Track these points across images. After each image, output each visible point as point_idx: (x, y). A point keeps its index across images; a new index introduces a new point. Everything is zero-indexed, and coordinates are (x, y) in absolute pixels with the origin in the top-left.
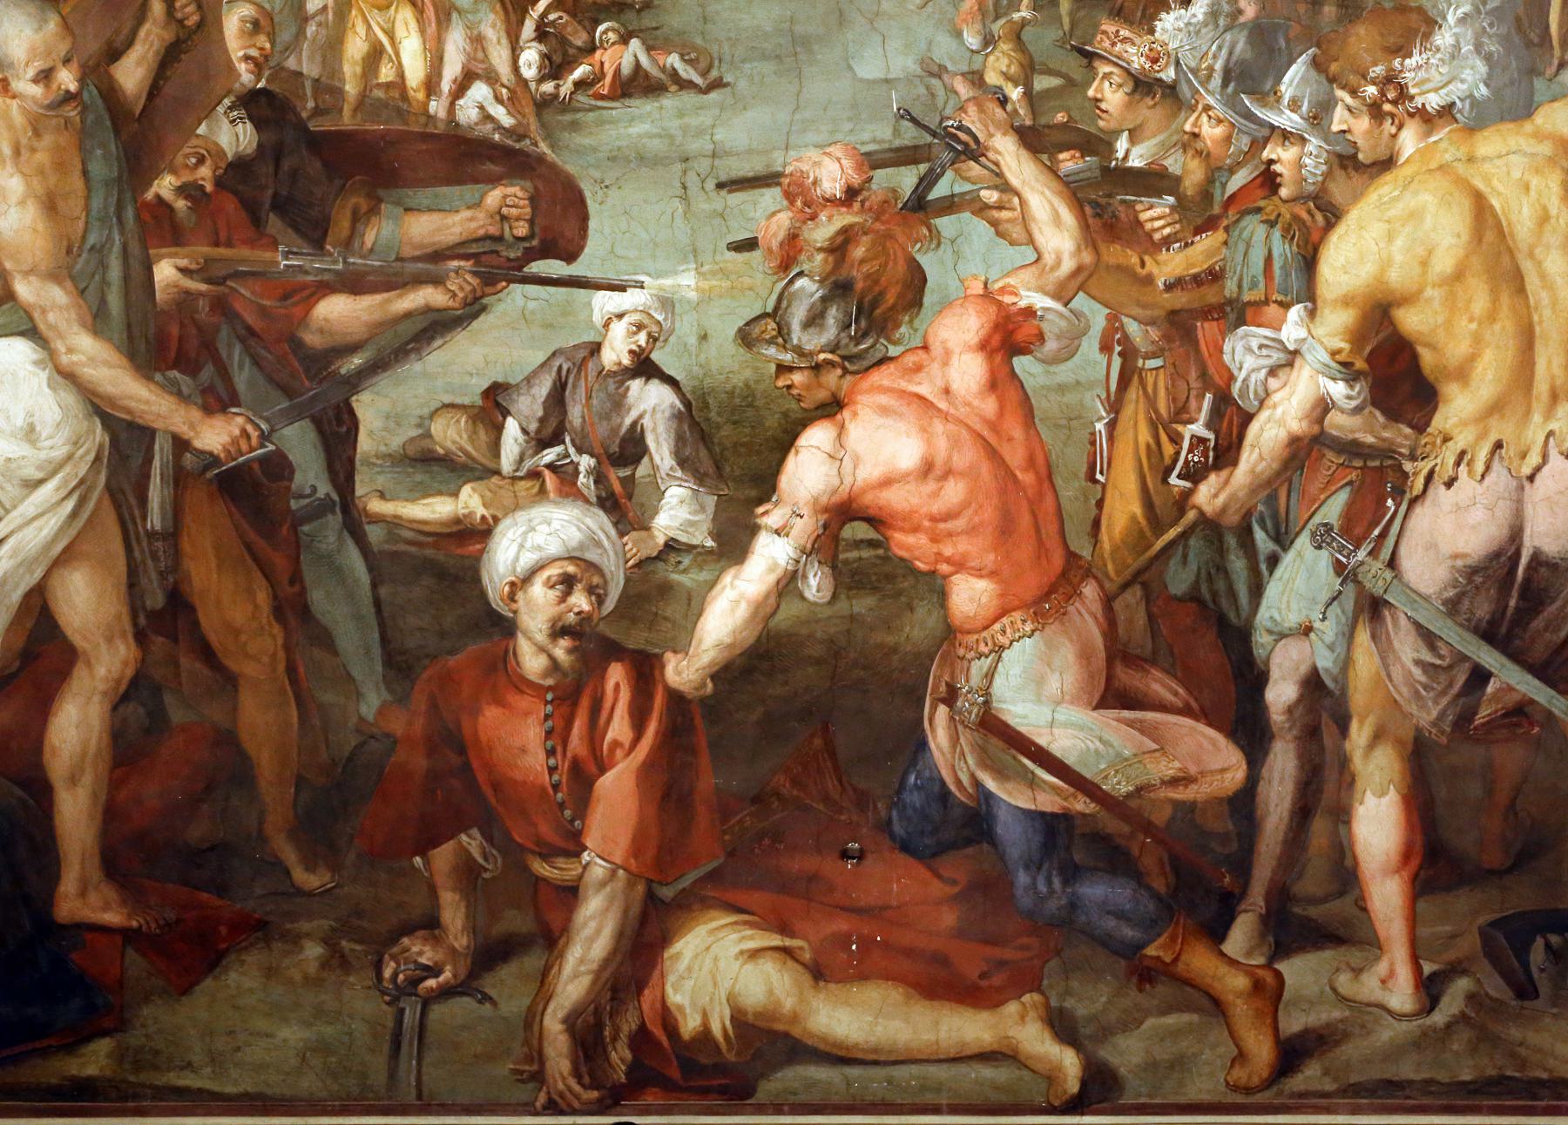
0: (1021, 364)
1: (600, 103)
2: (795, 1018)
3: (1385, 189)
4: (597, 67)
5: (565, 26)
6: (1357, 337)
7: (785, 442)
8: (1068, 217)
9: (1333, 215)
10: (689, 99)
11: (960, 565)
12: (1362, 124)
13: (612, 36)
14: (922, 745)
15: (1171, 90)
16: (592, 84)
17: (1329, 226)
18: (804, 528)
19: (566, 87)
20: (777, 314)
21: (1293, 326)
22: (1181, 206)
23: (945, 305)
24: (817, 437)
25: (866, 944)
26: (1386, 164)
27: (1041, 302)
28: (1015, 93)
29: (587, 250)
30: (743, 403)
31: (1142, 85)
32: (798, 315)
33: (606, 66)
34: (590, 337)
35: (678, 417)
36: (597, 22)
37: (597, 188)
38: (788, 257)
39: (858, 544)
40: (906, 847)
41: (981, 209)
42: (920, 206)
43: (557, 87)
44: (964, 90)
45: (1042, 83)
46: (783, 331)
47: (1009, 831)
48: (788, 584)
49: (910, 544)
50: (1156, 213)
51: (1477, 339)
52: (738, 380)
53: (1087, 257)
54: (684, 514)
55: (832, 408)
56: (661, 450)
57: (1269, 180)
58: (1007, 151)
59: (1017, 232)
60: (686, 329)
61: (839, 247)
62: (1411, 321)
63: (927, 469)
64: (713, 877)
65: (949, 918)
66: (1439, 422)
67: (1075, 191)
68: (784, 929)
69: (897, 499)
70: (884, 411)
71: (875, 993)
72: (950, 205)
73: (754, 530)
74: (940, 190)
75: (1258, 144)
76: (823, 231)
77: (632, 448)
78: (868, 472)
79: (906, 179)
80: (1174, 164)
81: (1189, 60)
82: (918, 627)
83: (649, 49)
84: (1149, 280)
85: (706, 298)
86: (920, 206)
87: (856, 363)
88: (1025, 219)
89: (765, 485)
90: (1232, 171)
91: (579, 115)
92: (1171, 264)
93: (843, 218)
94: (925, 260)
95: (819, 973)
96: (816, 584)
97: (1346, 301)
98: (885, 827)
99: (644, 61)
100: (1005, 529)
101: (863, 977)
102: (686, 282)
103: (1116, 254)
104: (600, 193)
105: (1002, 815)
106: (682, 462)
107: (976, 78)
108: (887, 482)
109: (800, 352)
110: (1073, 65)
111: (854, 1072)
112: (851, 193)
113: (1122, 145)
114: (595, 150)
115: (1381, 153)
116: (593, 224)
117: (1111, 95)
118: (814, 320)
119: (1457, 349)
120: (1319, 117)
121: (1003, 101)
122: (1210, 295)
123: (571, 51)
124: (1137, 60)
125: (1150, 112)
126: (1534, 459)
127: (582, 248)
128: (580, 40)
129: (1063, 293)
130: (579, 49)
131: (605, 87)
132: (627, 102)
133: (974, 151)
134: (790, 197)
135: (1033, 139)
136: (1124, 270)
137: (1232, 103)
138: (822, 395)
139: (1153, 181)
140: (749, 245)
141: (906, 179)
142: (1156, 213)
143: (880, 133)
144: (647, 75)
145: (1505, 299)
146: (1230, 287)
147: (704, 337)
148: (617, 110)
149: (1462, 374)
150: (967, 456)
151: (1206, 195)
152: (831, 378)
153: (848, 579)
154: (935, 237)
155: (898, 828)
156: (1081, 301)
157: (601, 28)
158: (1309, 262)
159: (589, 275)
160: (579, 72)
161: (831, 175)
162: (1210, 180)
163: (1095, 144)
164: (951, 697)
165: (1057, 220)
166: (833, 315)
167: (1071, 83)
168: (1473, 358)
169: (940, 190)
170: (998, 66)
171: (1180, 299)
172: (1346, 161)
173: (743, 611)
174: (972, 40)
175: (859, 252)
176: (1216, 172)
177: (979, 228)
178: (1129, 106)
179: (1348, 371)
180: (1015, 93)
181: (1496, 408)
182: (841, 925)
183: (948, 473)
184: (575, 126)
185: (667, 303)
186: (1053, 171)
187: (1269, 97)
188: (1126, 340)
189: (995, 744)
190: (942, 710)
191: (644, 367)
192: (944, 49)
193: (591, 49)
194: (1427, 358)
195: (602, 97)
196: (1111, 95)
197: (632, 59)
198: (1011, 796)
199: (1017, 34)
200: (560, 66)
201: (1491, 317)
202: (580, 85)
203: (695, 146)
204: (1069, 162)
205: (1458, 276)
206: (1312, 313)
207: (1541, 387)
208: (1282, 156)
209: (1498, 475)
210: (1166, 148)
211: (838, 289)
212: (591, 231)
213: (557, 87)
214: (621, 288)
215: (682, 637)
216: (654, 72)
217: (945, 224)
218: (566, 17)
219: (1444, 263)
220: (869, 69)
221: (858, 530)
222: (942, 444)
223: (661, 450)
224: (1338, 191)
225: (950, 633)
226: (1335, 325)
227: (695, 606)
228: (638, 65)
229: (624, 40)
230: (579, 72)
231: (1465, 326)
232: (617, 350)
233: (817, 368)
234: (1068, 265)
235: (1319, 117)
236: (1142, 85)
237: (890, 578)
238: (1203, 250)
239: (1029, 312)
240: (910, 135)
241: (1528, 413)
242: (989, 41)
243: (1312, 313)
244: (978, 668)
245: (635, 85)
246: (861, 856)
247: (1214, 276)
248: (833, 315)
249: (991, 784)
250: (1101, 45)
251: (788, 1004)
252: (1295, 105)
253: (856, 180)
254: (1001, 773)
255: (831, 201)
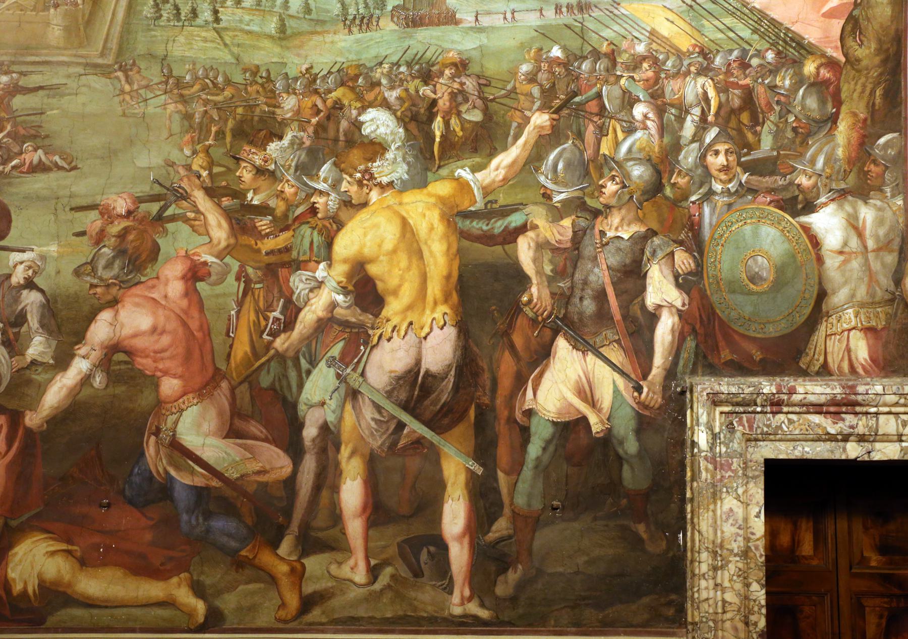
0: (200, 286)
1: (22, 175)
2: (70, 585)
3: (363, 215)
4: (23, 160)
5: (10, 144)
6: (350, 276)
7: (91, 317)
8: (225, 224)
9: (340, 225)
10: (62, 174)
11: (166, 373)
12: (354, 188)
13: (30, 148)
14: (142, 454)
15: (272, 174)
16: (19, 167)
17: (339, 230)
18: (96, 355)
19: (8, 168)
20: (92, 263)
21: (321, 272)
22: (275, 220)
23: (168, 260)
24: (105, 316)
25: (108, 549)
26: (365, 204)
27: (210, 259)
28: (205, 174)
29: (9, 235)
30: (73, 300)
31: (260, 171)
32: (102, 263)
33: (26, 161)
34: (6, 271)
35: (43, 306)
36: (24, 143)
37: (17, 209)
38: (99, 238)
39: (120, 363)
40: (131, 502)
41: (186, 220)
42: (160, 219)
43: (4, 168)
44: (182, 172)
45: (216, 170)
46: (94, 270)
47: (180, 495)
48: (86, 380)
49: (144, 363)
50: (263, 223)
51: (402, 278)
52: (72, 291)
53: (232, 241)
54: (41, 348)
55: (113, 303)
56: (33, 321)
57: (313, 210)
58: (200, 198)
59: (202, 230)
60: (50, 269)
61: (122, 235)
62: (373, 270)
63: (154, 330)
64: (37, 516)
65: (148, 536)
66: (385, 313)
67: (228, 214)
68: (69, 541)
69: (140, 343)
70: (137, 305)
71: (110, 573)
72: (173, 219)
73: (72, 356)
74: (169, 212)
75: (309, 196)
76: (116, 228)
77: (21, 319)
78: (127, 331)
79: (155, 208)
80: (272, 203)
81: (281, 162)
82: (145, 400)
83: (46, 154)
84: (259, 251)
85: (61, 256)
86: (160, 219)
87: (126, 284)
88: (206, 224)
89: (80, 336)
90: (297, 206)
91: (13, 180)
92: (269, 244)
93: (125, 223)
94: (160, 241)
95: (83, 563)
96: (99, 381)
97: (345, 261)
98: (122, 492)
99: (43, 158)
100: (188, 357)
101: (104, 564)
102: (53, 249)
103: (246, 240)
104: (18, 211)
105: (177, 488)
106: (42, 325)
107: (188, 168)
108: (135, 336)
109: (101, 279)
110: (231, 163)
111: (95, 611)
112: (129, 213)
113: (250, 195)
114: (17, 194)
115: (362, 201)
116: (13, 224)
117: (247, 175)
118: (109, 265)
119: (393, 282)
120: (335, 185)
121: (199, 177)
122: (285, 258)
123: (12, 154)
124: (258, 160)
125: (262, 182)
126: (426, 330)
127: (7, 234)
128: (16, 149)
129: (220, 256)
130: (15, 153)
131: (25, 169)
132: (34, 175)
133: (184, 196)
134: (102, 214)
135: (211, 192)
136: (249, 247)
137: (299, 179)
138: (109, 297)
139: (263, 210)
140: (83, 234)
141: (155, 208)
142: (263, 223)
143: (144, 189)
144: (44, 164)
145: (415, 261)
146: (294, 254)
147: (58, 272)
148: (30, 178)
149: (395, 293)
150: (173, 325)
151: (286, 216)
152: (114, 291)
153: (113, 378)
154: (165, 231)
155: (128, 493)
156: (228, 259)
157: (25, 145)
158: (329, 244)
159: (9, 245)
160: (13, 163)
161: (121, 206)
162: (288, 210)
163: (239, 195)
164: (157, 432)
165: (220, 225)
166: (117, 264)
167: (229, 169)
168: (400, 286)
169: (169, 212)
170: (198, 163)
171: (272, 259)
172: (347, 203)
173: (64, 392)
174: (187, 152)
175: (131, 237)
176: (290, 206)
177: (185, 228)
178: (255, 179)
179: (345, 291)
180: (205, 174)
181: (410, 307)
182: (97, 539)
183: (163, 332)
184: (10, 184)
185: (43, 258)
186: (219, 205)
187: (315, 177)
188: (247, 276)
189: (177, 455)
190: (153, 438)
191: (30, 284)
192: (175, 156)
193: (21, 153)
194: (380, 286)
195: (23, 173)
196: (247, 175)
197: (38, 158)
198: (182, 478)
199: (207, 150)
200: (6, 160)
201: (409, 268)
202: (14, 167)
203: (61, 193)
204: (226, 202)
205: (394, 251)
206: (330, 266)
207: (430, 298)
208: (320, 201)
209: (411, 336)
210: (269, 197)
211: (120, 252)
212: (12, 228)
213: (4, 168)
214: (23, 251)
215: (34, 405)
216: (47, 163)
217: (170, 226)
218: (11, 141)
219: (388, 246)
220: (143, 161)
221: (121, 357)
222: (162, 319)
223: (33, 321)
224: (343, 215)
225: (159, 403)
226: (340, 271)
227: (42, 389)
228: (40, 160)
229: (35, 150)
230: (13, 163)
231: (397, 272)
232: (18, 277)
233: (108, 286)
234: (223, 244)
235: (335, 185)
236: (260, 171)
237: (132, 378)
238: (283, 239)
239: (205, 263)
240: (157, 189)
241: (424, 309)
242: (195, 152)
243: (330, 266)
244: (171, 419)
245: (39, 168)
246: (109, 506)
247: (287, 249)
248: (117, 264)
249: (173, 473)
250: (243, 155)
251: (67, 577)
252: (325, 180)
253: (132, 207)
254: (178, 468)
255: (120, 216)
